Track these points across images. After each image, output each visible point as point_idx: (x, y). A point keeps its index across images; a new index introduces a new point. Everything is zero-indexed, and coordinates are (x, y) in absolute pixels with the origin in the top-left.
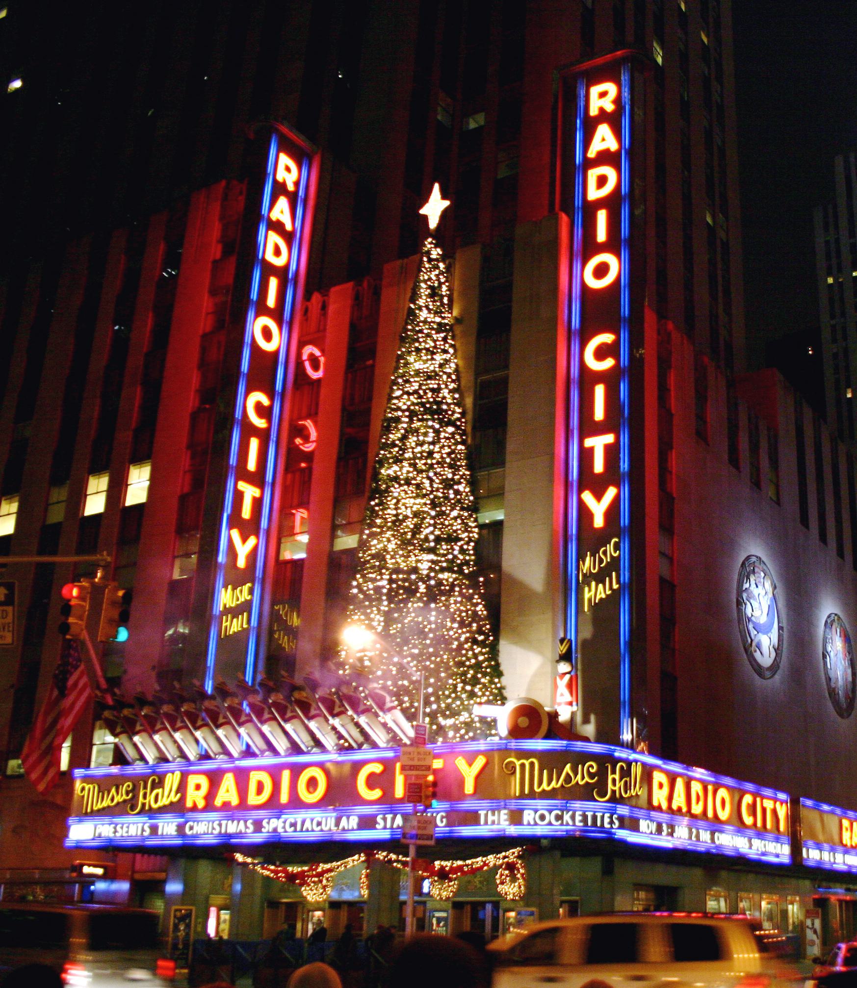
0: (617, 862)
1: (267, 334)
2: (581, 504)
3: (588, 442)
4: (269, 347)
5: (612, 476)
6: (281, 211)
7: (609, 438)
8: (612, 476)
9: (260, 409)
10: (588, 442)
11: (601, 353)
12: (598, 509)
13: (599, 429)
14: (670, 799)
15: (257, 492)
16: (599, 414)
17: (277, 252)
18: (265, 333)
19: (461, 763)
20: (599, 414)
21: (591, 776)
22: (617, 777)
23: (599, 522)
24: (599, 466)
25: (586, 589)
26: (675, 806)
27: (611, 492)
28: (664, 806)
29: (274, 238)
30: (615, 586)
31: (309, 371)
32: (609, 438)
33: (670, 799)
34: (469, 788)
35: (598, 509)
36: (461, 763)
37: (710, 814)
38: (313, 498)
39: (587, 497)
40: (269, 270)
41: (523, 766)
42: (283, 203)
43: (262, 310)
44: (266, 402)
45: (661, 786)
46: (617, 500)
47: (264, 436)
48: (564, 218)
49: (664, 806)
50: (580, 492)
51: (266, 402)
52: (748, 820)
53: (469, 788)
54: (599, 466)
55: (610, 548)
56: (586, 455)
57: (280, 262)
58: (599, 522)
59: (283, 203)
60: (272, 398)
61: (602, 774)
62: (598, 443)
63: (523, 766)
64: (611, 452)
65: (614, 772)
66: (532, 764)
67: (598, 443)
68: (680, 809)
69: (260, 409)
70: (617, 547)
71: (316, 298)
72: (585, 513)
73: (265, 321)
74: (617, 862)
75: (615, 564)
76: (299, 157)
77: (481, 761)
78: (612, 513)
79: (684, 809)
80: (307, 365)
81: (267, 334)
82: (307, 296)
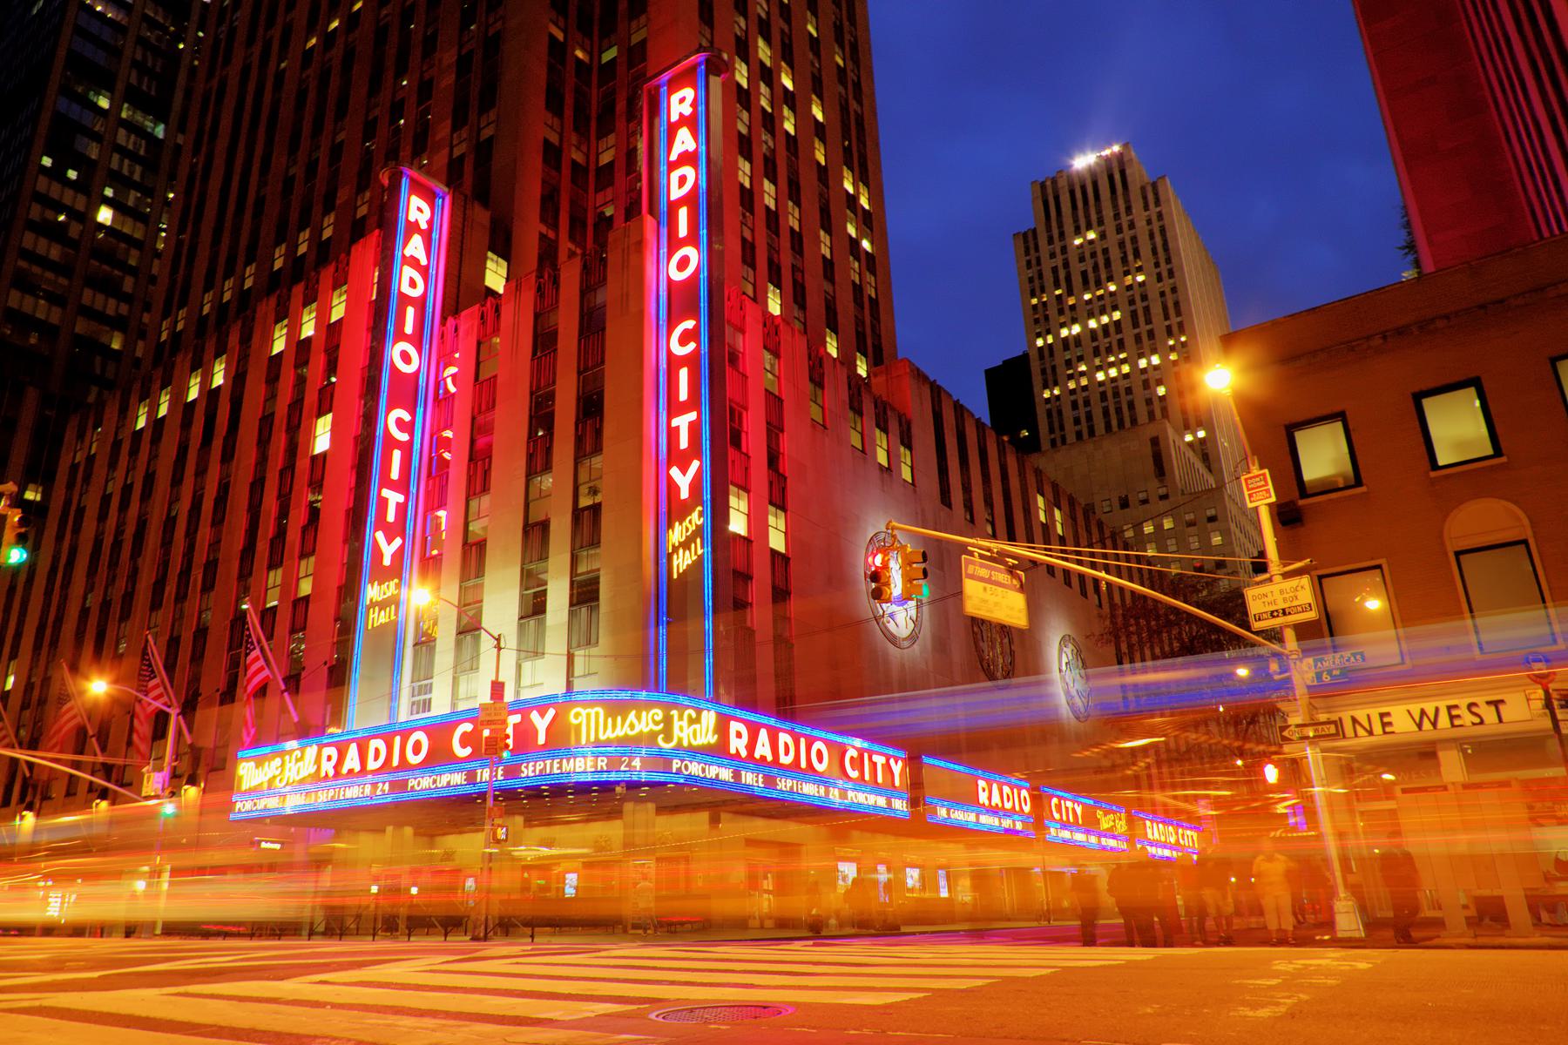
0: (724, 816)
1: (406, 357)
2: (670, 478)
3: (675, 422)
4: (408, 369)
6: (415, 247)
7: (693, 416)
8: (695, 450)
9: (400, 423)
10: (675, 422)
12: (683, 481)
13: (683, 409)
14: (751, 746)
15: (401, 498)
16: (683, 395)
17: (413, 284)
18: (403, 357)
19: (534, 716)
20: (683, 395)
21: (656, 723)
22: (685, 723)
23: (684, 494)
24: (684, 443)
26: (757, 756)
27: (695, 464)
28: (744, 753)
29: (408, 272)
30: (700, 552)
31: (452, 389)
32: (693, 416)
33: (751, 746)
34: (541, 740)
35: (683, 481)
36: (534, 716)
37: (803, 765)
38: (449, 500)
39: (675, 472)
40: (405, 300)
41: (588, 716)
42: (417, 240)
43: (400, 336)
44: (407, 417)
45: (739, 735)
47: (407, 448)
48: (649, 221)
49: (744, 753)
51: (407, 417)
52: (854, 774)
53: (541, 740)
54: (684, 443)
55: (695, 516)
56: (673, 433)
57: (416, 293)
58: (684, 494)
59: (417, 240)
60: (413, 414)
61: (668, 721)
62: (683, 422)
63: (588, 716)
64: (694, 428)
65: (681, 718)
66: (597, 714)
67: (683, 422)
68: (763, 758)
69: (400, 423)
70: (701, 514)
71: (450, 322)
72: (673, 487)
73: (403, 346)
74: (724, 816)
75: (699, 531)
76: (430, 196)
77: (551, 713)
78: (695, 486)
79: (770, 758)
80: (449, 381)
81: (406, 357)
82: (444, 319)
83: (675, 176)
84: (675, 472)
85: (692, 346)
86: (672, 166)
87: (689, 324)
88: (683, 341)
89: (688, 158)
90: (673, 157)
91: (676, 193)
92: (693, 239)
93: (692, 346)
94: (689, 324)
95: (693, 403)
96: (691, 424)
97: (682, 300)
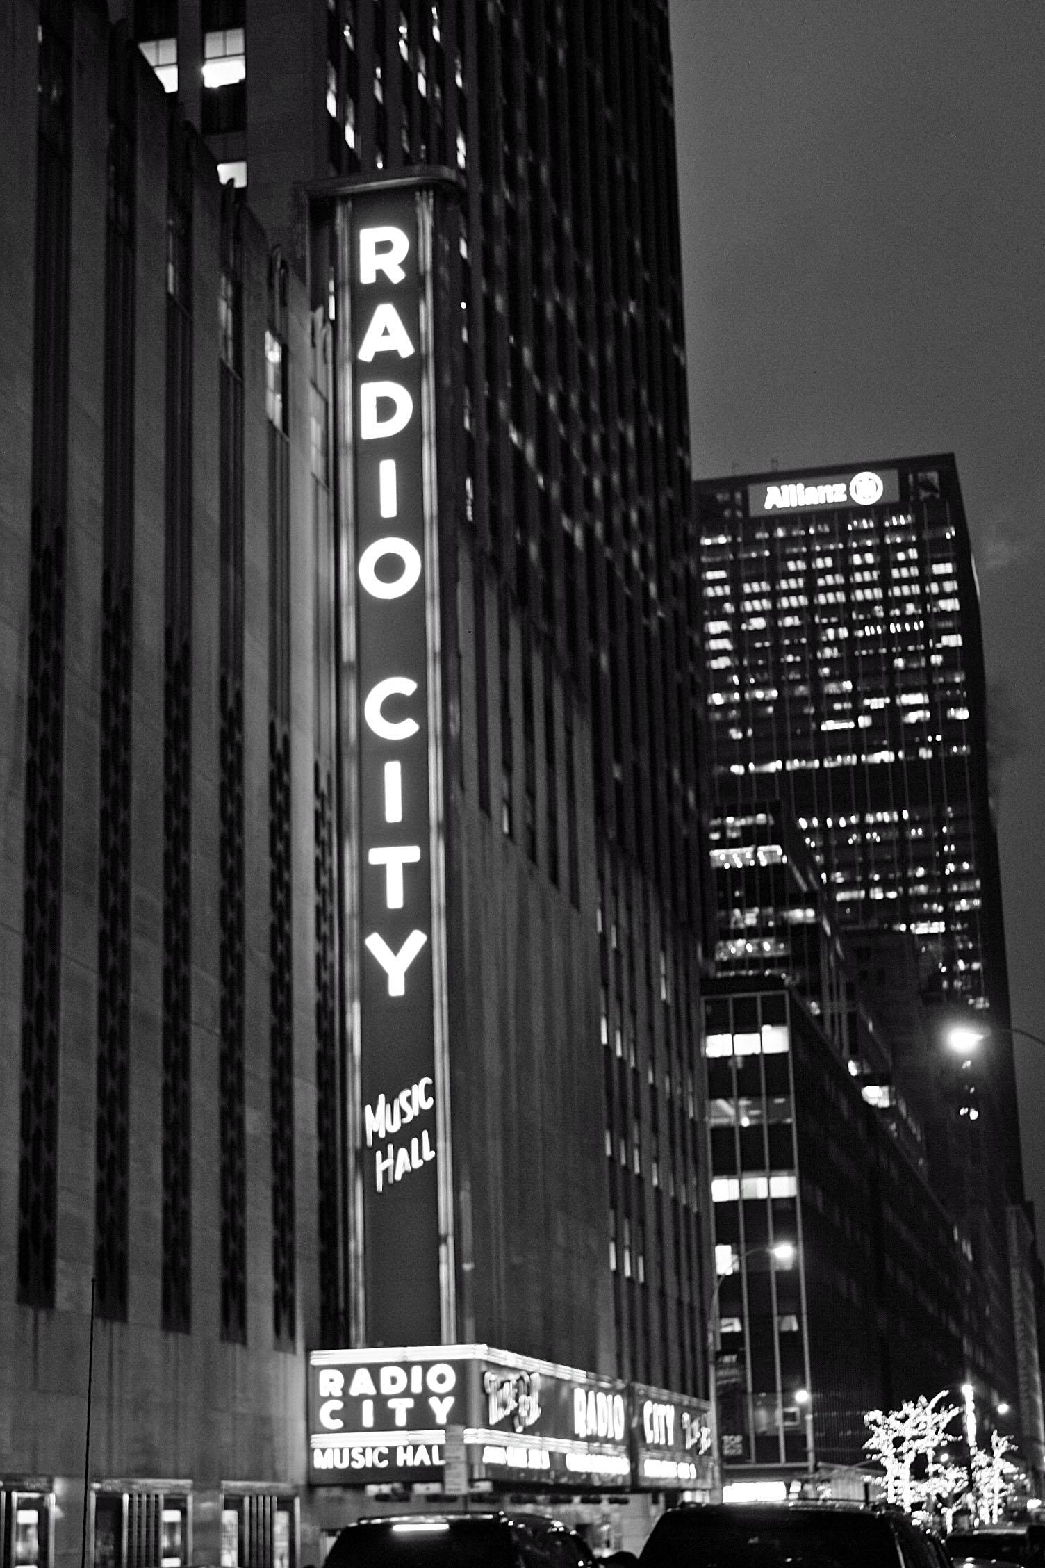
3: (376, 856)
5: (416, 913)
7: (412, 854)
8: (416, 913)
10: (376, 856)
11: (395, 709)
13: (394, 836)
16: (394, 812)
23: (396, 987)
24: (395, 898)
25: (379, 1154)
27: (416, 940)
32: (412, 854)
39: (376, 944)
46: (426, 955)
50: (363, 934)
54: (395, 898)
56: (373, 878)
58: (396, 987)
62: (393, 859)
64: (416, 875)
72: (373, 975)
83: (371, 391)
84: (376, 944)
85: (407, 729)
86: (362, 373)
87: (405, 686)
88: (395, 709)
89: (387, 366)
90: (366, 354)
91: (372, 429)
92: (408, 523)
93: (407, 729)
94: (405, 686)
95: (412, 829)
96: (408, 868)
97: (391, 635)
